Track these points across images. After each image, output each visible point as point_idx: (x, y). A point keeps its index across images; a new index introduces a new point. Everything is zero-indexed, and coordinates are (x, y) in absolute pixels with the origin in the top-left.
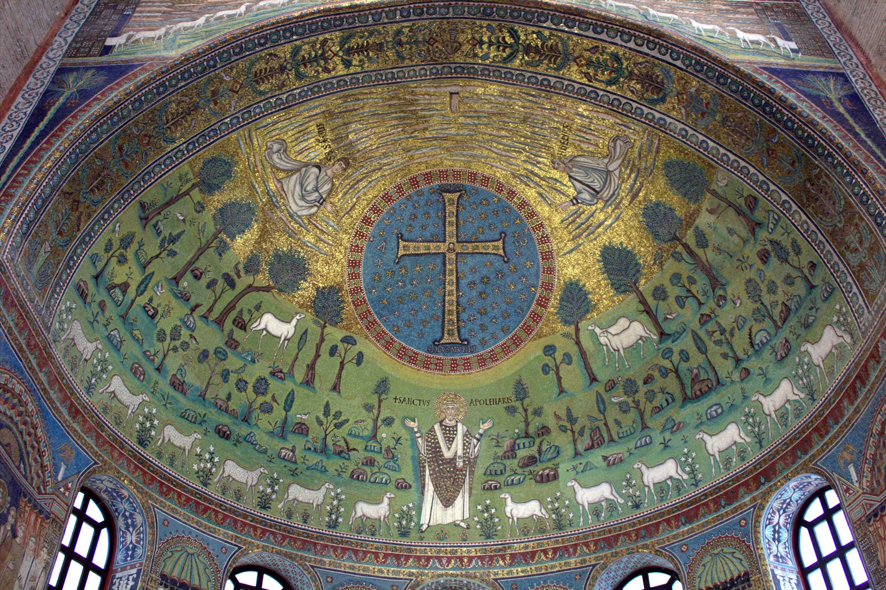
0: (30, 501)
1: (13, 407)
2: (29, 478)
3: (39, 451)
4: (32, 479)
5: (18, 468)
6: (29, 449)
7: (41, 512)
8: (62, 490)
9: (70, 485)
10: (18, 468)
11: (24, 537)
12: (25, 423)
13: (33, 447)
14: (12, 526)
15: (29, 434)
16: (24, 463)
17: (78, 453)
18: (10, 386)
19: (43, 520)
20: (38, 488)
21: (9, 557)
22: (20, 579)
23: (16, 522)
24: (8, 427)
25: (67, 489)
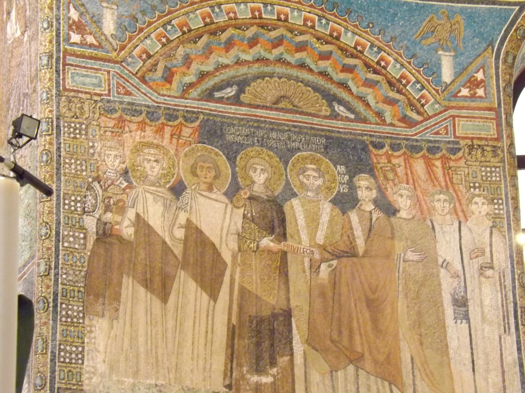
0: (395, 147)
1: (253, 42)
2: (370, 116)
3: (367, 65)
4: (379, 114)
5: (335, 116)
6: (342, 76)
7: (433, 150)
8: (465, 92)
9: (480, 76)
10: (335, 116)
11: (418, 202)
12: (301, 47)
13: (348, 69)
14: (375, 202)
15: (325, 56)
16: (341, 102)
17: (470, 17)
18: (221, 19)
19: (445, 160)
20: (404, 119)
21: (399, 246)
22: (446, 265)
23: (381, 190)
24: (262, 76)
25: (474, 84)
